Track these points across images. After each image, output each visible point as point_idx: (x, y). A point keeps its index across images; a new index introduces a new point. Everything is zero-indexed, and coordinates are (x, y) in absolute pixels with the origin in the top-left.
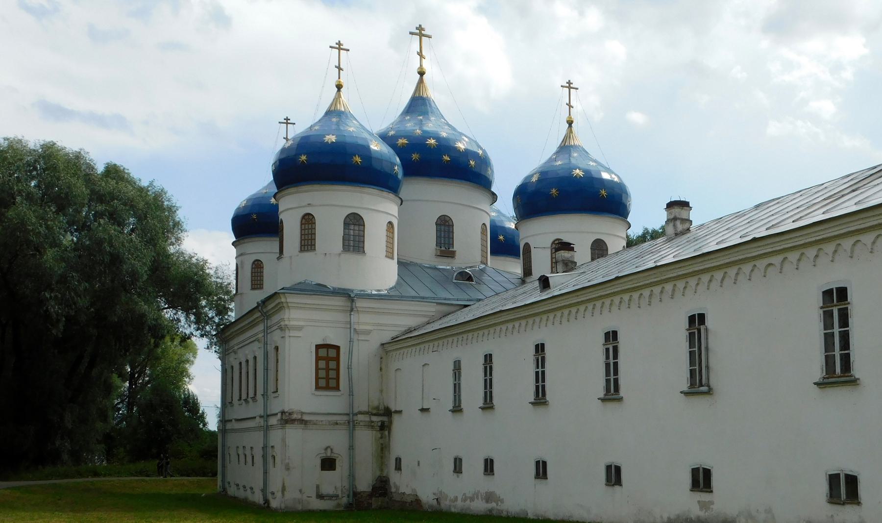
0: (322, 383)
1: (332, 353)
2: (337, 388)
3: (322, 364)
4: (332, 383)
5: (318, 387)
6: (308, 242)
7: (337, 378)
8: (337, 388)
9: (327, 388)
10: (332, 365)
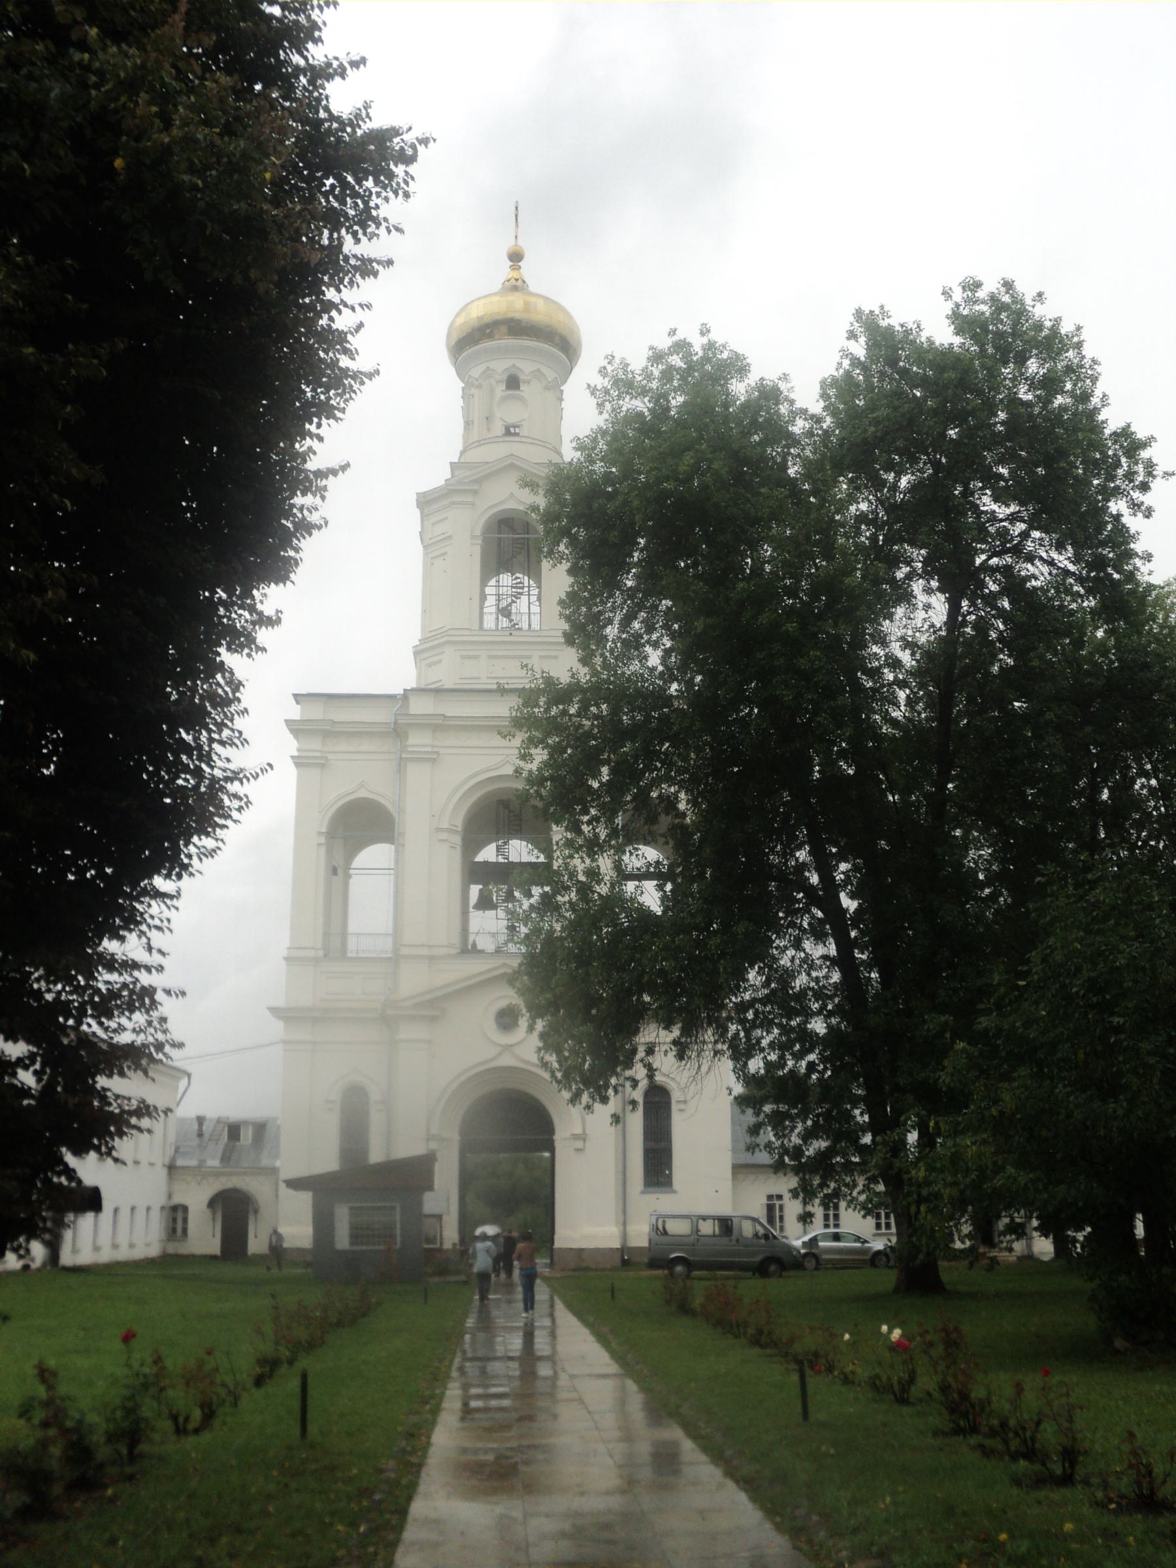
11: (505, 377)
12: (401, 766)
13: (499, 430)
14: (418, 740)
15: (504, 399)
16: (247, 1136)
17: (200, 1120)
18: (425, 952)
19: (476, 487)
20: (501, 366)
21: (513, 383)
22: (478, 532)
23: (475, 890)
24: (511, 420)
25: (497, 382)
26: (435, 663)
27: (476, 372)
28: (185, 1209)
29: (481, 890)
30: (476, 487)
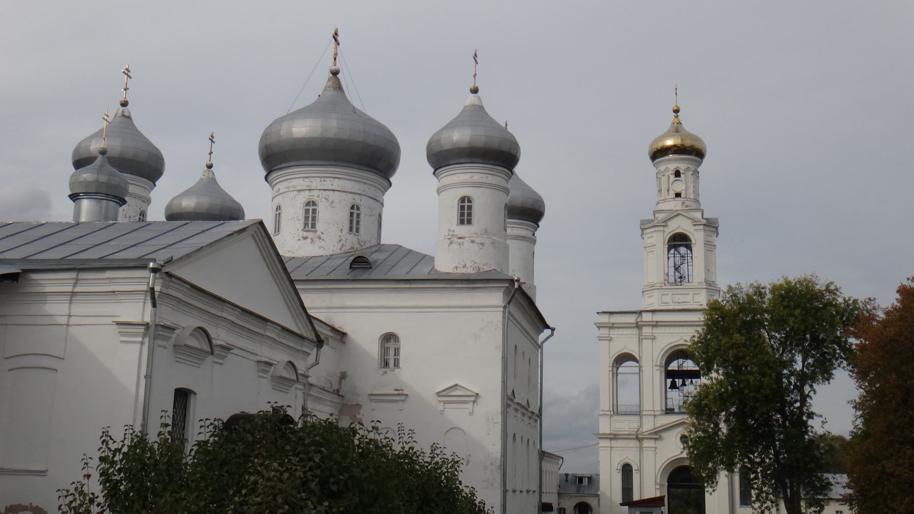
12: (640, 341)
13: (672, 195)
14: (646, 331)
16: (585, 482)
17: (567, 475)
18: (652, 413)
19: (664, 224)
20: (673, 166)
21: (677, 174)
22: (666, 241)
23: (669, 381)
24: (678, 190)
25: (671, 174)
26: (651, 296)
27: (662, 168)
28: (564, 509)
29: (671, 382)
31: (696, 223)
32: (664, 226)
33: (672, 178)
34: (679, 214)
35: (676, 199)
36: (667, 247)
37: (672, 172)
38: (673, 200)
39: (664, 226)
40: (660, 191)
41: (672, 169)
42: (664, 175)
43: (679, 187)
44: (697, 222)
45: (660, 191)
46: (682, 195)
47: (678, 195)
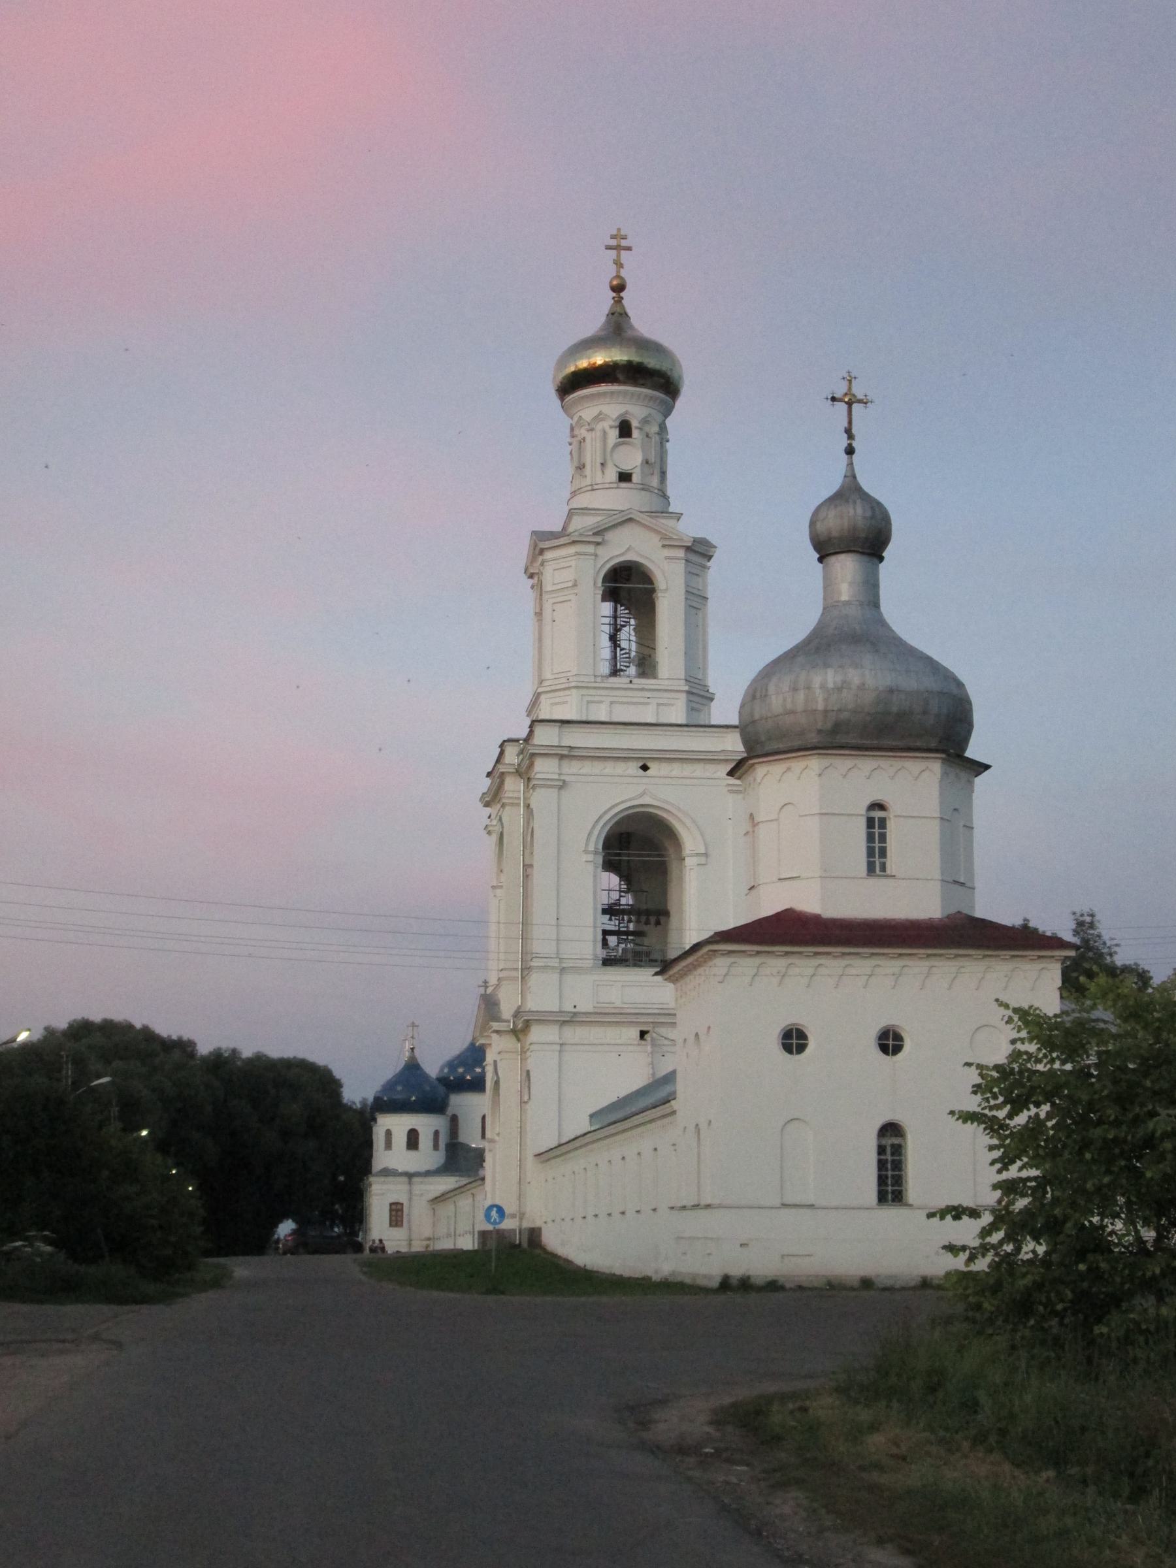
0: (394, 1223)
1: (399, 1207)
2: (402, 1225)
3: (394, 1213)
4: (399, 1223)
5: (391, 1225)
6: (388, 1145)
7: (402, 1221)
8: (402, 1225)
9: (396, 1225)
10: (399, 1213)
11: (617, 423)
13: (612, 475)
15: (616, 445)
19: (598, 539)
21: (625, 429)
24: (626, 467)
25: (611, 427)
27: (588, 413)
30: (598, 539)
31: (668, 543)
32: (598, 544)
33: (613, 434)
34: (630, 520)
35: (623, 485)
36: (601, 592)
37: (613, 424)
38: (615, 485)
39: (598, 544)
40: (581, 467)
41: (614, 417)
42: (592, 430)
43: (631, 457)
44: (671, 539)
45: (581, 467)
46: (635, 478)
47: (625, 477)
